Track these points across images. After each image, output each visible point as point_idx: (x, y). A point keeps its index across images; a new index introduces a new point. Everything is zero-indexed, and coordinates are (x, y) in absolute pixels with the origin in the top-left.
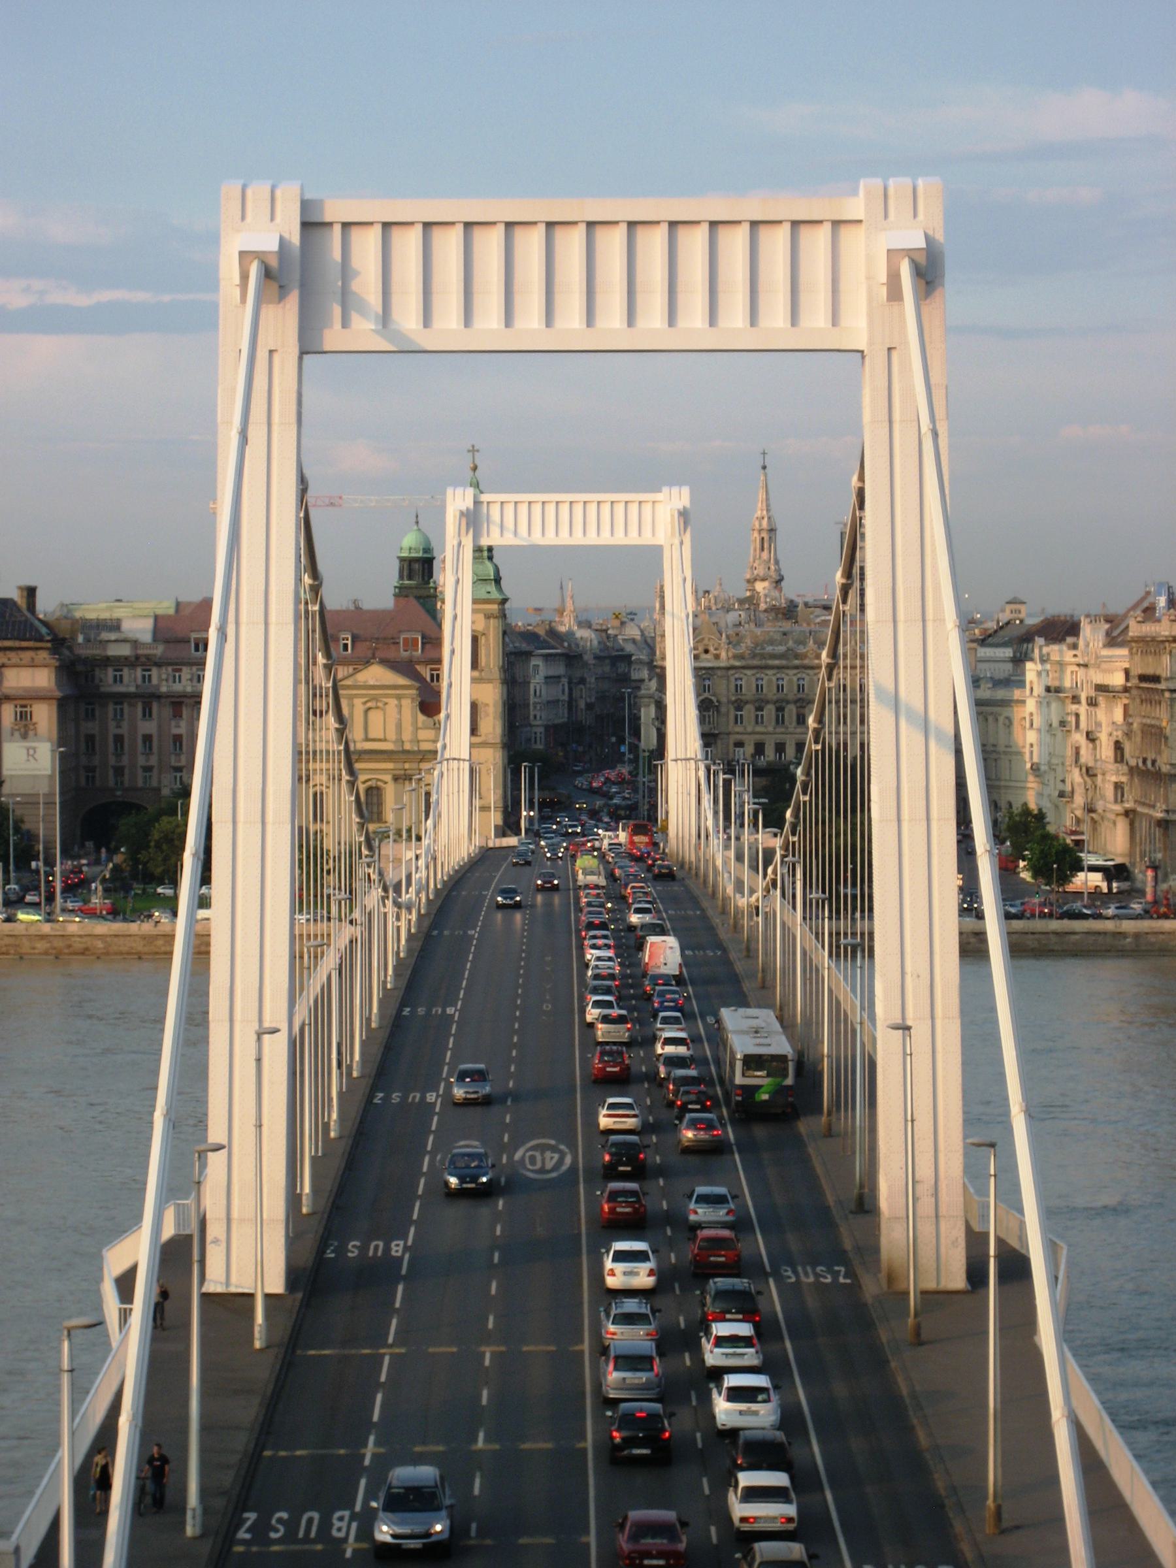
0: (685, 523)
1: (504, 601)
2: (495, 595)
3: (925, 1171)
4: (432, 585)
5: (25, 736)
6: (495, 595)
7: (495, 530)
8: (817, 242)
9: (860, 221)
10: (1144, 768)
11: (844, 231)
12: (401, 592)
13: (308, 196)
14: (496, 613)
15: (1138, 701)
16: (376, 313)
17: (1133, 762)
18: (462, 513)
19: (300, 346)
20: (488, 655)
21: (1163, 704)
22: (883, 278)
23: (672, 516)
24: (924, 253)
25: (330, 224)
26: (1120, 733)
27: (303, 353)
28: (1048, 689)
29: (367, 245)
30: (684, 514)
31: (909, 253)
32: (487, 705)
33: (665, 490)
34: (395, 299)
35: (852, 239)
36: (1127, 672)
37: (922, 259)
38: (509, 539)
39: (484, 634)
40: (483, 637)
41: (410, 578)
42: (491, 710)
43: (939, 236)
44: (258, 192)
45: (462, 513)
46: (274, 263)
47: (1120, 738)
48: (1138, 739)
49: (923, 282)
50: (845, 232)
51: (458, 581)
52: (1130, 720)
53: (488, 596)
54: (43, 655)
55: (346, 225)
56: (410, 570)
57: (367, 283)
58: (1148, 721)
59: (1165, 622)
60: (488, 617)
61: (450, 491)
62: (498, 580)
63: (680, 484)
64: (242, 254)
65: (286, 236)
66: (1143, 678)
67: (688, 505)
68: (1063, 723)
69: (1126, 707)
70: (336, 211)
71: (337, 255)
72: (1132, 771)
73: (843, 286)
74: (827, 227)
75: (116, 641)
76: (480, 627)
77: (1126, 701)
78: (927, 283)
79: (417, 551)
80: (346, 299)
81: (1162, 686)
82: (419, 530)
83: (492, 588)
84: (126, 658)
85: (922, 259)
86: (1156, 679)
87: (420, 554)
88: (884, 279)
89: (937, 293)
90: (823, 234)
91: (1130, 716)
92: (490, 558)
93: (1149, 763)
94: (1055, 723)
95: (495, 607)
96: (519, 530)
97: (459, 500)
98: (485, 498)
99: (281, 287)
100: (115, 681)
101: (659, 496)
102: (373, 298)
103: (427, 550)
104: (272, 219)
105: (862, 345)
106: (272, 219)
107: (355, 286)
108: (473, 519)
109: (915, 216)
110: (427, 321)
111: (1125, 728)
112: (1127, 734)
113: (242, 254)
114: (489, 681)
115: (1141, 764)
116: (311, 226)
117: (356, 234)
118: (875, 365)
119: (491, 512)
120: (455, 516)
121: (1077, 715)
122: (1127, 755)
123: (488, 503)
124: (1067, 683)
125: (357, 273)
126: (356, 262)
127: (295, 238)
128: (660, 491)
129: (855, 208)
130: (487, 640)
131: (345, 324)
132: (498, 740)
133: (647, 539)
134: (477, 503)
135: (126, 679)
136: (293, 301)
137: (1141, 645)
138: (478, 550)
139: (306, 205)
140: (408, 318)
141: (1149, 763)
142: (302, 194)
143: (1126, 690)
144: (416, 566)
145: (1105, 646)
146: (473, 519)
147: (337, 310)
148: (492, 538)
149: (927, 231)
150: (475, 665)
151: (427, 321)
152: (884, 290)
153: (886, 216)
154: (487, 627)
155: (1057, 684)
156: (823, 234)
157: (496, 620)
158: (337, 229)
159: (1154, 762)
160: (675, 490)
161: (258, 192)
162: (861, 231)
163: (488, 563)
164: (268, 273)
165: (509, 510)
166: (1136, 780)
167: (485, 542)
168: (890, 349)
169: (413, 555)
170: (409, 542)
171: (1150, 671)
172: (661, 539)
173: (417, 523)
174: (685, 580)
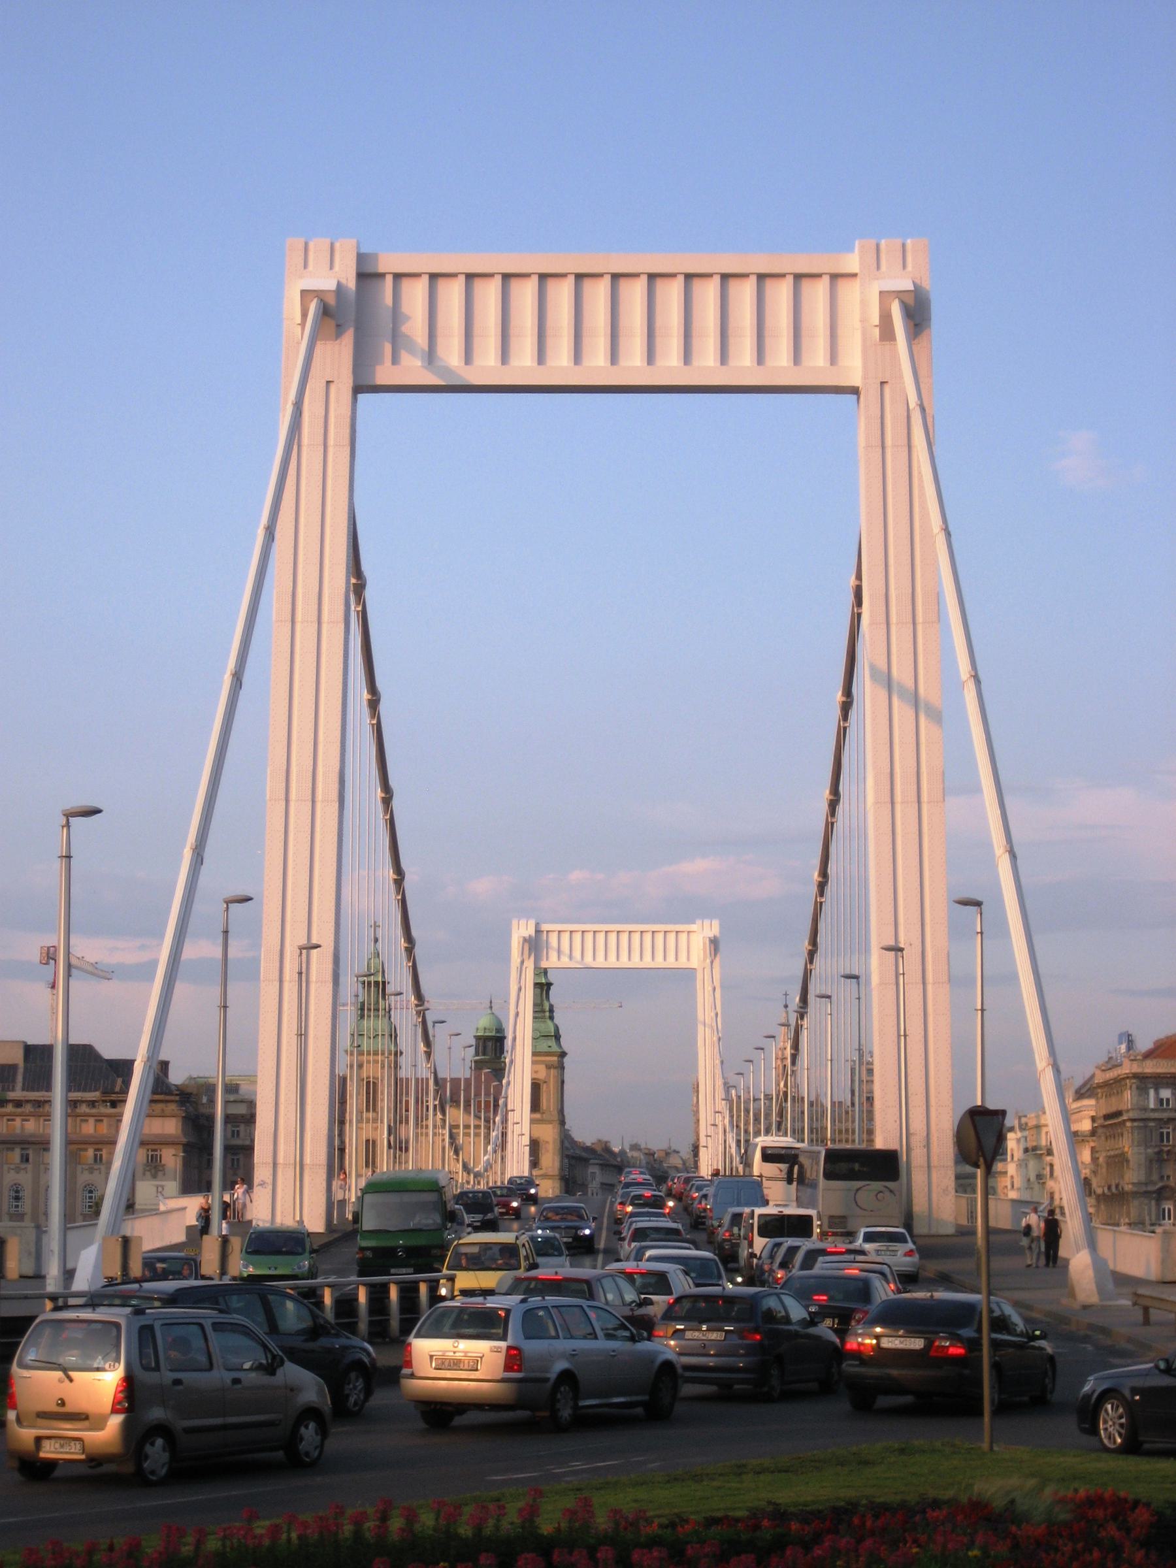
0: (715, 950)
1: (563, 1054)
2: (555, 1048)
3: (918, 1124)
4: (503, 1060)
5: (154, 1177)
6: (555, 1048)
7: (553, 955)
8: (817, 293)
9: (855, 275)
10: (1109, 1194)
11: (842, 284)
12: (478, 1065)
13: (362, 251)
14: (556, 1064)
15: (1103, 1138)
16: (423, 350)
17: (1099, 1191)
18: (525, 940)
19: (354, 381)
20: (548, 1100)
21: (1125, 1134)
22: (876, 320)
23: (704, 944)
24: (913, 295)
25: (382, 276)
26: (1087, 1171)
27: (358, 389)
28: (1026, 1150)
29: (415, 295)
30: (714, 943)
31: (898, 294)
32: (547, 1142)
33: (699, 922)
34: (441, 342)
35: (850, 293)
36: (1093, 1119)
37: (910, 301)
38: (565, 961)
39: (545, 1082)
40: (545, 1085)
41: (484, 1054)
42: (551, 1147)
43: (926, 284)
44: (318, 246)
45: (525, 940)
46: (331, 301)
47: (1088, 1176)
48: (1104, 1170)
49: (912, 324)
50: (843, 286)
51: (520, 989)
52: (1097, 1155)
53: (549, 1050)
54: (172, 1107)
55: (398, 277)
56: (485, 1048)
57: (416, 326)
58: (1112, 1153)
59: (1126, 1063)
60: (549, 1067)
61: (515, 922)
62: (557, 1037)
63: (711, 916)
64: (304, 293)
65: (344, 281)
66: (1107, 1117)
67: (718, 934)
68: (1039, 1177)
69: (1093, 1149)
70: (388, 263)
71: (388, 299)
72: (1101, 1199)
73: (841, 331)
74: (826, 280)
75: (235, 1101)
76: (542, 1074)
77: (1092, 1144)
78: (916, 325)
79: (490, 1030)
80: (397, 339)
81: (1125, 1117)
82: (493, 1014)
83: (552, 1042)
84: (242, 1116)
85: (910, 301)
86: (1118, 1114)
87: (493, 1034)
88: (876, 321)
89: (925, 333)
90: (822, 286)
91: (1097, 1152)
92: (551, 1018)
93: (1114, 1190)
94: (1033, 1178)
95: (555, 1058)
96: (574, 954)
97: (522, 929)
98: (545, 927)
99: (338, 326)
100: (233, 1136)
101: (693, 927)
102: (421, 339)
103: (500, 1030)
104: (331, 267)
105: (856, 380)
106: (331, 267)
107: (405, 329)
108: (535, 945)
109: (904, 267)
110: (468, 358)
111: (1092, 1167)
112: (1094, 1172)
113: (304, 293)
114: (550, 1122)
115: (1106, 1191)
116: (367, 276)
117: (406, 284)
118: (870, 396)
119: (550, 940)
120: (519, 943)
121: (1052, 1166)
122: (1094, 1185)
123: (548, 932)
124: (1043, 1143)
125: (408, 318)
126: (405, 308)
127: (351, 284)
128: (694, 923)
129: (852, 262)
130: (548, 1087)
131: (395, 360)
132: (556, 1172)
133: (683, 962)
134: (538, 932)
135: (242, 1134)
136: (348, 338)
137: (1106, 1089)
138: (536, 968)
139: (361, 258)
140: (451, 354)
141: (1114, 1190)
142: (358, 247)
143: (1093, 1133)
144: (490, 1044)
145: (1074, 1101)
146: (535, 945)
147: (388, 348)
148: (551, 961)
149: (916, 281)
150: (535, 1106)
151: (468, 358)
152: (877, 331)
153: (878, 268)
154: (548, 1075)
155: (1035, 1144)
156: (822, 286)
157: (556, 1071)
158: (389, 279)
159: (1117, 1186)
160: (707, 922)
161: (318, 246)
162: (856, 285)
163: (549, 1022)
164: (326, 311)
165: (566, 937)
166: (1102, 1207)
167: (544, 964)
168: (882, 383)
169: (486, 1034)
170: (483, 1023)
171: (1113, 1109)
172: (694, 963)
173: (491, 1007)
174: (714, 989)
